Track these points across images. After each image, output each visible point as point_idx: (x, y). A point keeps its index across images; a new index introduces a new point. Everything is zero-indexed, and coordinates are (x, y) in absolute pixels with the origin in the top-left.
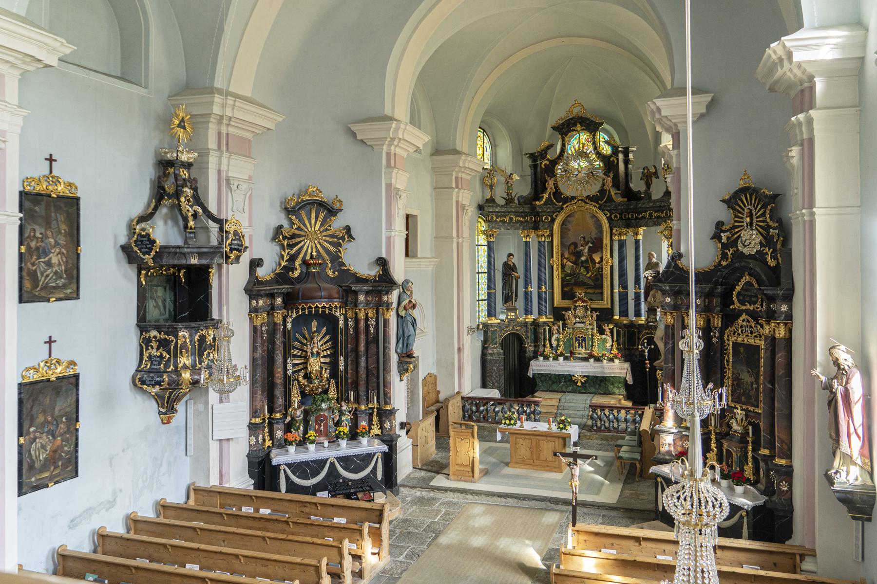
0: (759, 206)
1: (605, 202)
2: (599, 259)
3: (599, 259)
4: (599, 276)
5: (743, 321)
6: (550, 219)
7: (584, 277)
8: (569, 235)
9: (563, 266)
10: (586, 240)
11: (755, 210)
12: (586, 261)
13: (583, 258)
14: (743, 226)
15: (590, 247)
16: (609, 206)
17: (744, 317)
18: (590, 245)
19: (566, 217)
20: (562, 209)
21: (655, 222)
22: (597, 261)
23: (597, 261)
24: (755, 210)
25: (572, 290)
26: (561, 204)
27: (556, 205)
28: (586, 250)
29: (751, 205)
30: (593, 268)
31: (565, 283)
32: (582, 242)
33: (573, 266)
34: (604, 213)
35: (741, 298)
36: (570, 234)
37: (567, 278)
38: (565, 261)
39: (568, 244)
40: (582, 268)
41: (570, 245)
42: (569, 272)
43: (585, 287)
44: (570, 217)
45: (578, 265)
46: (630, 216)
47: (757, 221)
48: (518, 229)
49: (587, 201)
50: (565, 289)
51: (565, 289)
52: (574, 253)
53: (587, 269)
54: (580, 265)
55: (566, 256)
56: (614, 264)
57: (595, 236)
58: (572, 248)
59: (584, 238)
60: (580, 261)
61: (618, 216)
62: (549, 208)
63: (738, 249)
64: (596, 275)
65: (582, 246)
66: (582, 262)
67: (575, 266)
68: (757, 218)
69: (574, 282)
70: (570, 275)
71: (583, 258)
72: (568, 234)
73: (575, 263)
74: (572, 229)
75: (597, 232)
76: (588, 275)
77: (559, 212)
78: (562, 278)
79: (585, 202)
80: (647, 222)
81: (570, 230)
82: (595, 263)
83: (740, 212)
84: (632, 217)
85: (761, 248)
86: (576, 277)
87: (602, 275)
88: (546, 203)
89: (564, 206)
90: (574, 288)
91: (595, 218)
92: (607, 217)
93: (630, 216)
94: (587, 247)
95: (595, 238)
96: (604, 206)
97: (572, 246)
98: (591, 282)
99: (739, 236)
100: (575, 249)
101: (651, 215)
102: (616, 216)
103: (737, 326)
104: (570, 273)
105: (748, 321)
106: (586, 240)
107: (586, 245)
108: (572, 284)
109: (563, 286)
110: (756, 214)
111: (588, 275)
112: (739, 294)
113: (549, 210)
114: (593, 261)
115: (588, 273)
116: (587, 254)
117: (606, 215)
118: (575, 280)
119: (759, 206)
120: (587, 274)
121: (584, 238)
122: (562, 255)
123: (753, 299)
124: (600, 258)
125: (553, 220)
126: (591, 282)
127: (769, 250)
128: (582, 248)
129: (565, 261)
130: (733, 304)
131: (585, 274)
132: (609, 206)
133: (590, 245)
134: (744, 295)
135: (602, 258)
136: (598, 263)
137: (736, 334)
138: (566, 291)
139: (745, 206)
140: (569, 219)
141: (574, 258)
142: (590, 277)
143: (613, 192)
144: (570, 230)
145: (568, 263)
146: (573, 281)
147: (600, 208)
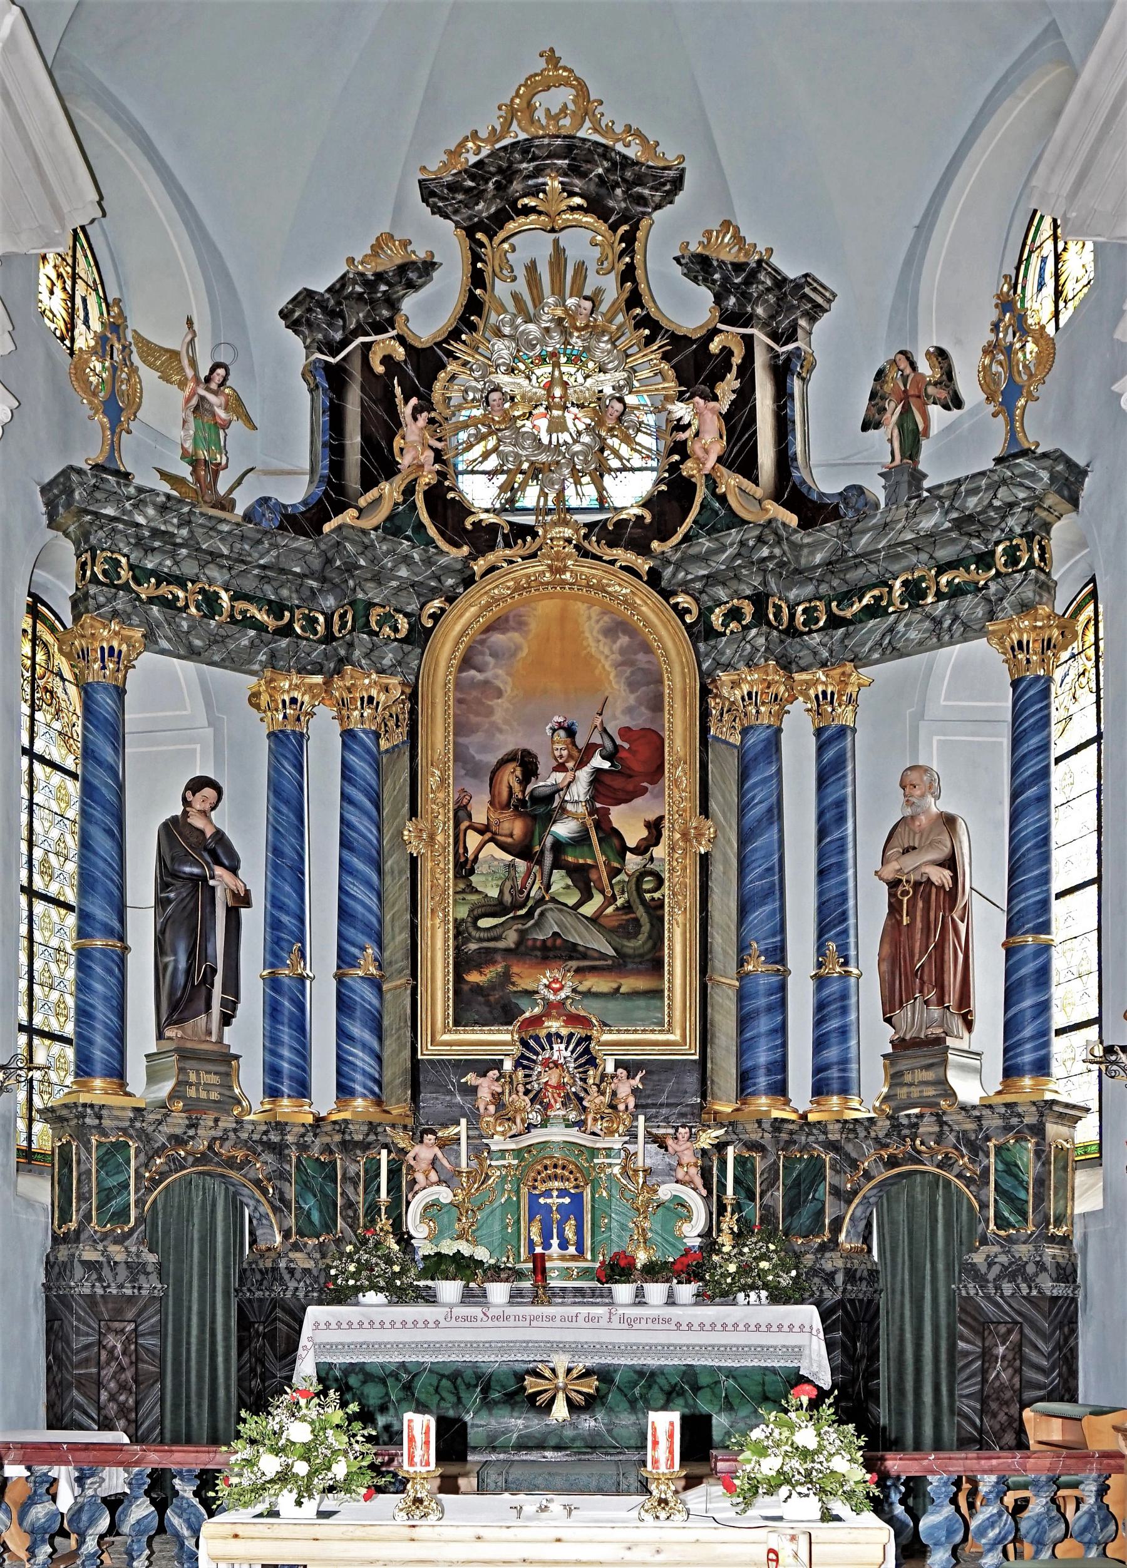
1: (687, 538)
2: (645, 833)
3: (645, 833)
4: (640, 912)
6: (403, 624)
7: (568, 920)
8: (498, 717)
9: (464, 868)
10: (581, 741)
12: (581, 840)
13: (563, 829)
15: (598, 771)
16: (704, 558)
18: (598, 762)
19: (489, 629)
20: (468, 581)
21: (937, 622)
22: (631, 843)
23: (631, 843)
25: (506, 977)
26: (466, 550)
27: (441, 552)
28: (580, 789)
30: (614, 873)
31: (473, 946)
32: (561, 748)
33: (511, 866)
34: (675, 607)
36: (501, 708)
37: (485, 923)
38: (473, 840)
39: (493, 759)
40: (557, 874)
41: (503, 763)
42: (494, 893)
43: (574, 964)
44: (504, 631)
45: (540, 862)
46: (800, 618)
48: (236, 663)
49: (593, 547)
50: (473, 977)
51: (473, 977)
52: (522, 802)
53: (582, 878)
54: (548, 859)
55: (480, 816)
56: (717, 856)
57: (625, 721)
58: (510, 776)
59: (571, 732)
60: (549, 841)
61: (748, 609)
62: (407, 560)
64: (627, 908)
65: (561, 768)
66: (559, 846)
67: (521, 865)
69: (520, 943)
70: (497, 908)
71: (563, 829)
72: (490, 712)
73: (523, 850)
74: (508, 690)
75: (632, 699)
76: (588, 909)
77: (450, 600)
78: (458, 924)
79: (586, 554)
80: (891, 630)
81: (499, 693)
82: (623, 849)
84: (811, 619)
86: (530, 914)
87: (656, 910)
88: (393, 527)
89: (480, 565)
90: (515, 969)
91: (624, 640)
92: (689, 627)
93: (800, 618)
94: (584, 775)
95: (625, 732)
96: (678, 566)
97: (511, 767)
98: (601, 944)
100: (525, 781)
101: (914, 592)
102: (734, 614)
104: (500, 900)
106: (581, 741)
107: (581, 764)
108: (507, 951)
109: (462, 964)
111: (588, 909)
113: (403, 572)
114: (611, 836)
115: (587, 897)
116: (581, 809)
117: (681, 613)
118: (522, 933)
120: (580, 904)
121: (571, 732)
122: (461, 812)
124: (648, 825)
125: (419, 636)
126: (601, 944)
128: (559, 777)
129: (473, 840)
131: (571, 902)
132: (704, 558)
133: (598, 762)
135: (655, 828)
136: (632, 851)
138: (477, 989)
140: (497, 638)
141: (516, 828)
142: (594, 920)
143: (731, 482)
144: (499, 693)
145: (491, 849)
146: (511, 938)
147: (654, 579)
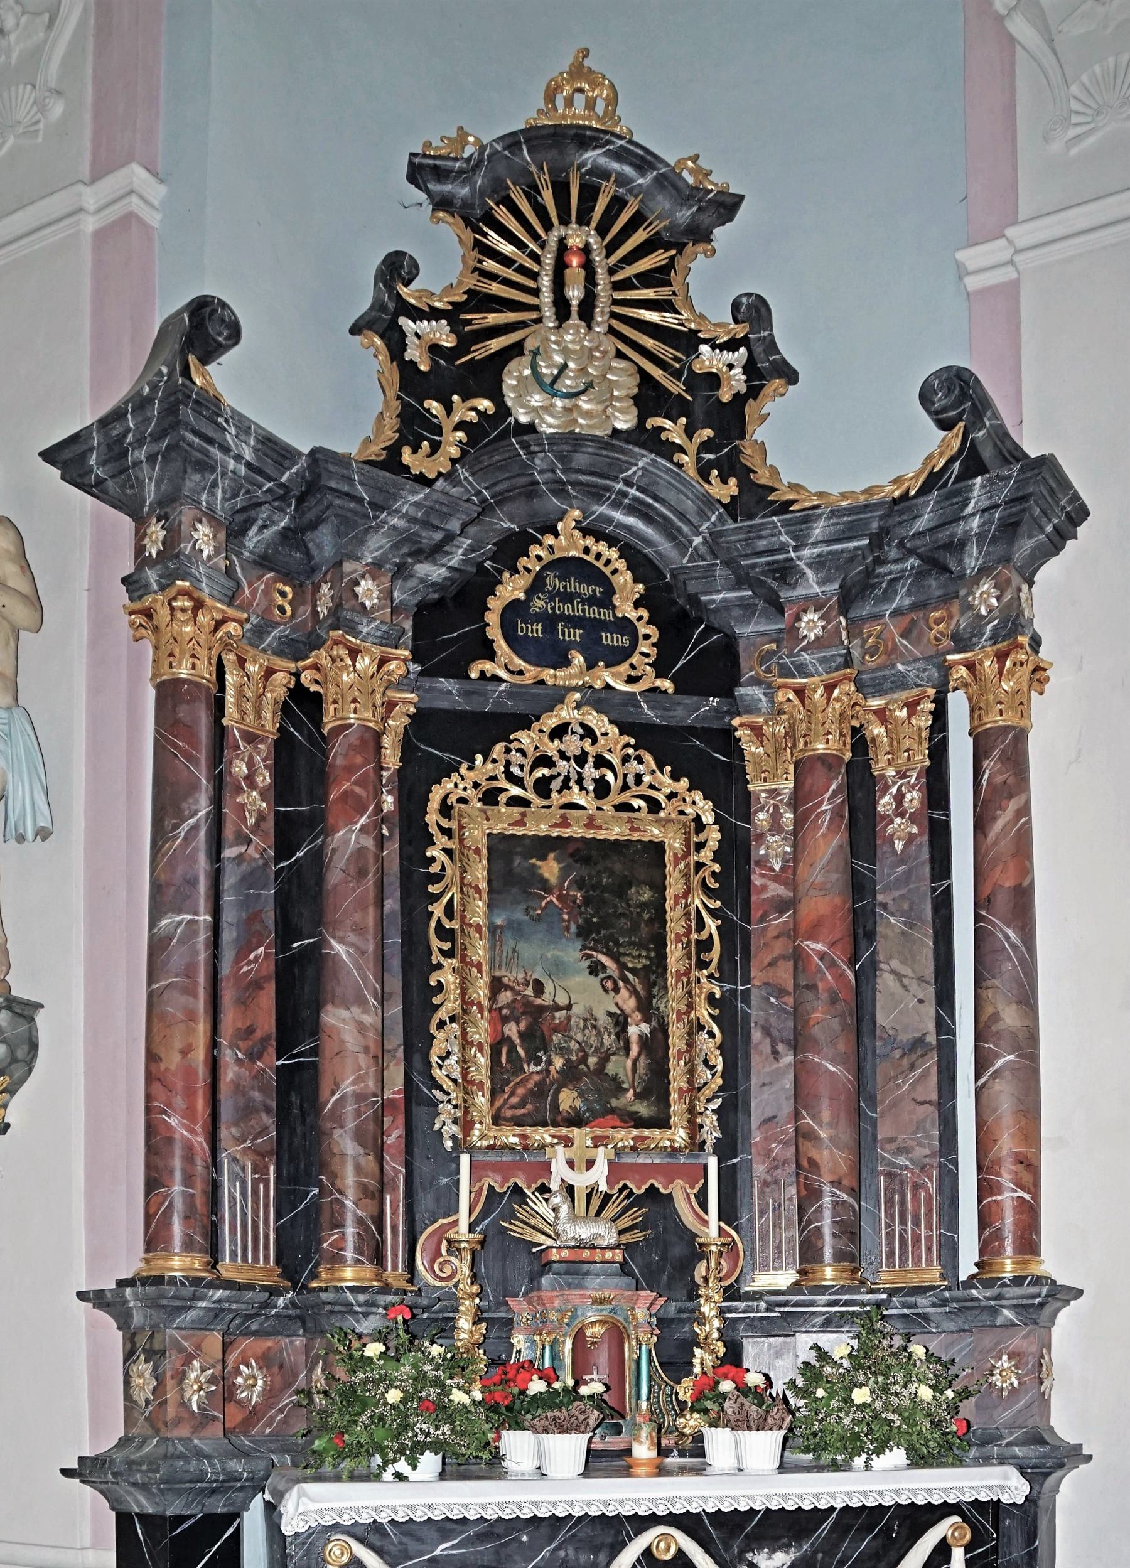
0: (640, 236)
5: (559, 732)
11: (610, 249)
14: (536, 308)
17: (565, 713)
24: (610, 249)
29: (584, 220)
35: (536, 630)
47: (616, 302)
63: (504, 412)
68: (618, 286)
83: (535, 237)
85: (642, 419)
99: (517, 349)
103: (515, 757)
105: (589, 733)
110: (612, 271)
112: (514, 611)
119: (640, 236)
123: (607, 638)
127: (689, 432)
130: (491, 656)
134: (550, 621)
137: (503, 798)
139: (548, 226)
